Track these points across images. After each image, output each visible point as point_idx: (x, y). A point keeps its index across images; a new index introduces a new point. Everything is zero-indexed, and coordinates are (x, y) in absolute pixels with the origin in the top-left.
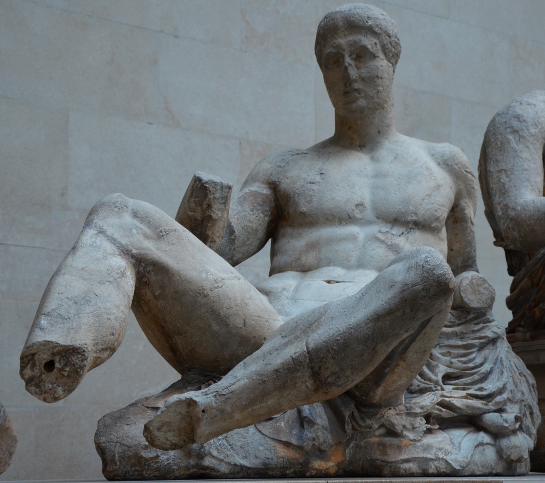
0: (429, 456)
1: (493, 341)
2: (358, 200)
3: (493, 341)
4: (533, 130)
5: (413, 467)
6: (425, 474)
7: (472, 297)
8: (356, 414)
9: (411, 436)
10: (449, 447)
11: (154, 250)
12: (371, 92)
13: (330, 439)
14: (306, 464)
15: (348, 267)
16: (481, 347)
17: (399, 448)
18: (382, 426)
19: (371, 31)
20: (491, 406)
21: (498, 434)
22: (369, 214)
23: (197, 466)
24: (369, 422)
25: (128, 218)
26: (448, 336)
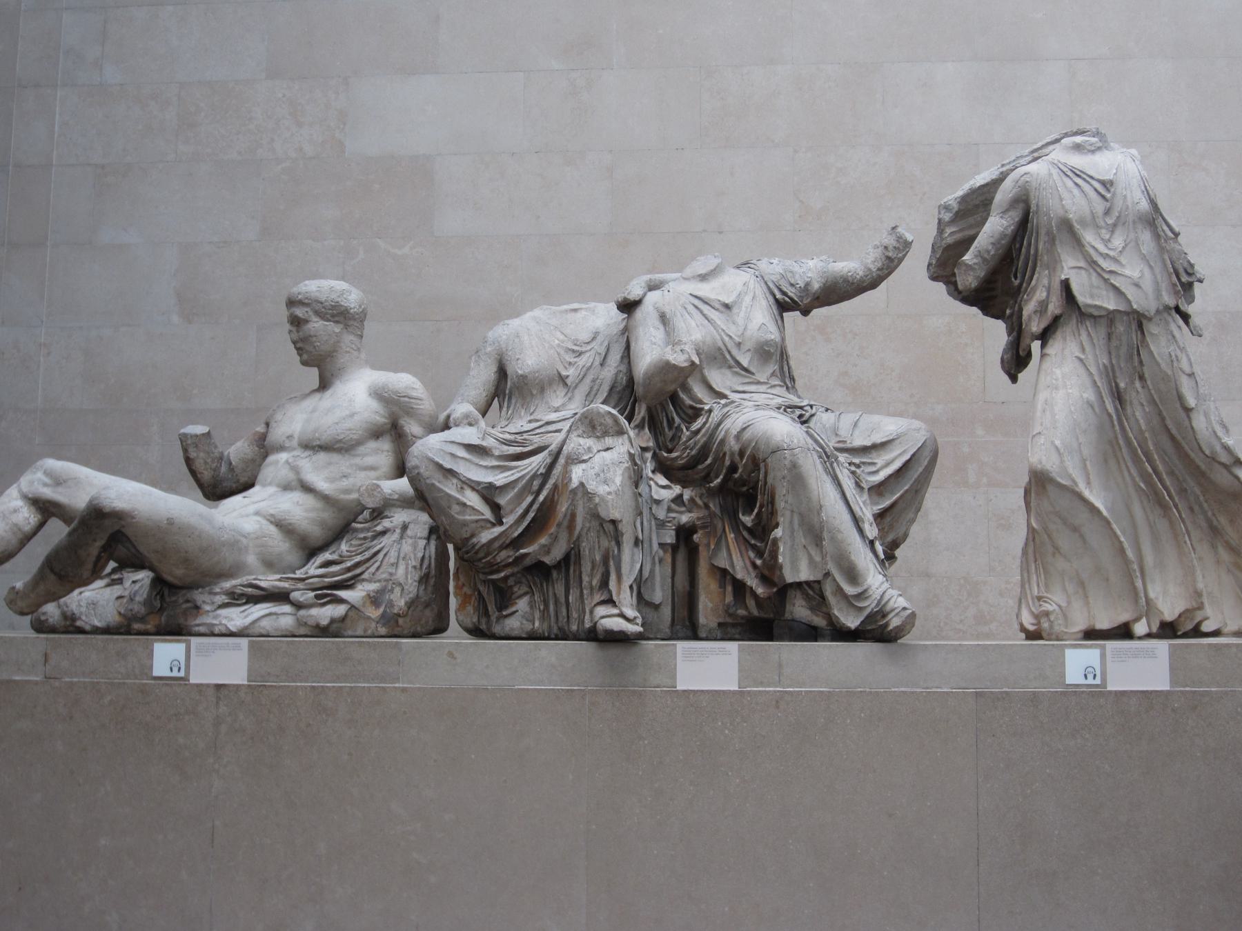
0: (215, 622)
1: (384, 533)
2: (290, 433)
3: (384, 533)
4: (489, 349)
5: (202, 629)
6: (213, 635)
7: (368, 500)
8: (166, 592)
9: (207, 608)
10: (234, 616)
11: (48, 493)
12: (310, 348)
13: (143, 610)
14: (129, 625)
15: (264, 486)
16: (374, 538)
17: (196, 616)
18: (187, 601)
19: (301, 303)
20: (300, 585)
21: (298, 606)
22: (295, 443)
23: (72, 625)
24: (174, 599)
25: (40, 475)
26: (362, 530)
